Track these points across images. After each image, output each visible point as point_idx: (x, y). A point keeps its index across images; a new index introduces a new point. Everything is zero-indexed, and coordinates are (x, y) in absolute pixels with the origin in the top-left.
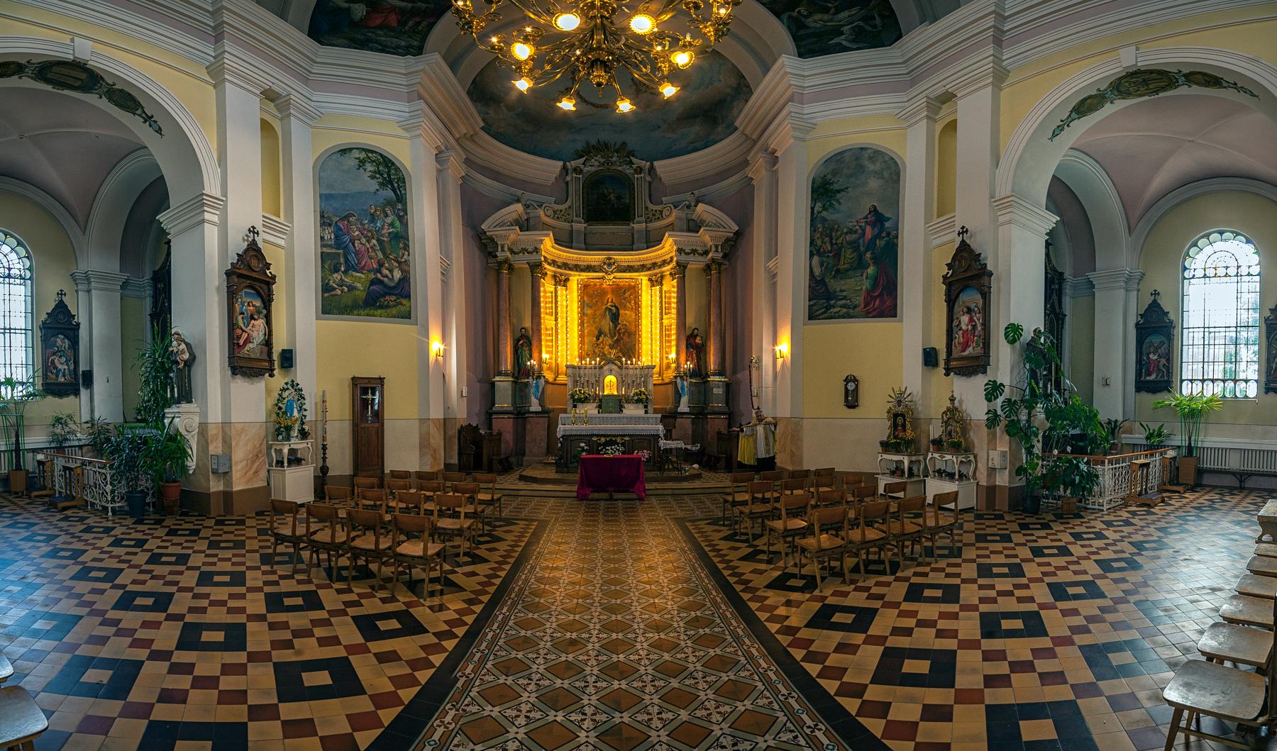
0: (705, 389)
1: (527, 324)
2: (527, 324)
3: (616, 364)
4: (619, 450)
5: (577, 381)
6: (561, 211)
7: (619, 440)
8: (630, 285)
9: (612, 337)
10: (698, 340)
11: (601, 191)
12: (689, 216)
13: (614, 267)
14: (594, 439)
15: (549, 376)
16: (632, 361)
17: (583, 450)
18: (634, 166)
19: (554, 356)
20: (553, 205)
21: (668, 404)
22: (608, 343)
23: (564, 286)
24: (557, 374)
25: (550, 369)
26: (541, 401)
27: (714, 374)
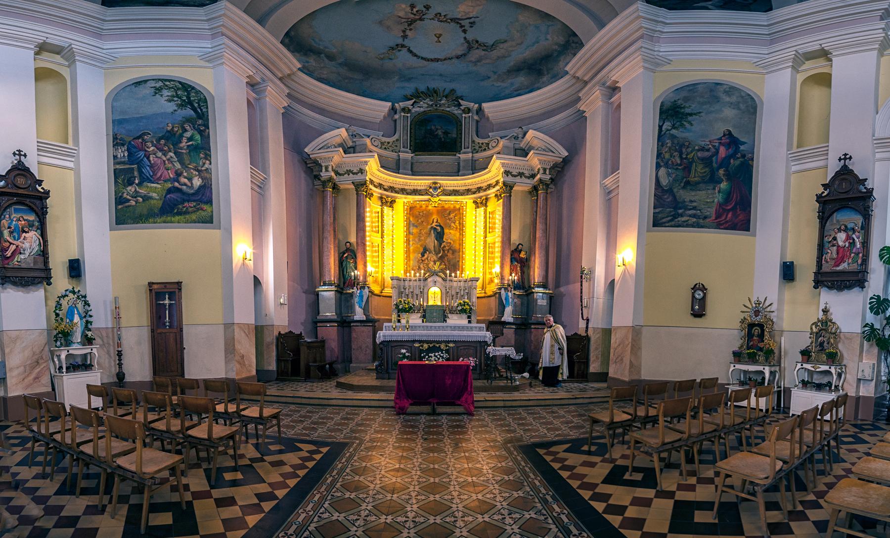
0: (528, 301)
1: (353, 239)
2: (353, 239)
3: (440, 277)
4: (443, 357)
5: (402, 293)
6: (389, 143)
7: (443, 346)
8: (454, 207)
9: (437, 254)
10: (522, 255)
11: (429, 128)
12: (517, 146)
13: (439, 191)
14: (417, 345)
15: (376, 289)
16: (456, 274)
17: (404, 357)
18: (462, 108)
19: (380, 270)
20: (381, 137)
21: (491, 316)
22: (432, 259)
23: (390, 207)
24: (383, 287)
25: (376, 281)
26: (366, 310)
27: (538, 287)
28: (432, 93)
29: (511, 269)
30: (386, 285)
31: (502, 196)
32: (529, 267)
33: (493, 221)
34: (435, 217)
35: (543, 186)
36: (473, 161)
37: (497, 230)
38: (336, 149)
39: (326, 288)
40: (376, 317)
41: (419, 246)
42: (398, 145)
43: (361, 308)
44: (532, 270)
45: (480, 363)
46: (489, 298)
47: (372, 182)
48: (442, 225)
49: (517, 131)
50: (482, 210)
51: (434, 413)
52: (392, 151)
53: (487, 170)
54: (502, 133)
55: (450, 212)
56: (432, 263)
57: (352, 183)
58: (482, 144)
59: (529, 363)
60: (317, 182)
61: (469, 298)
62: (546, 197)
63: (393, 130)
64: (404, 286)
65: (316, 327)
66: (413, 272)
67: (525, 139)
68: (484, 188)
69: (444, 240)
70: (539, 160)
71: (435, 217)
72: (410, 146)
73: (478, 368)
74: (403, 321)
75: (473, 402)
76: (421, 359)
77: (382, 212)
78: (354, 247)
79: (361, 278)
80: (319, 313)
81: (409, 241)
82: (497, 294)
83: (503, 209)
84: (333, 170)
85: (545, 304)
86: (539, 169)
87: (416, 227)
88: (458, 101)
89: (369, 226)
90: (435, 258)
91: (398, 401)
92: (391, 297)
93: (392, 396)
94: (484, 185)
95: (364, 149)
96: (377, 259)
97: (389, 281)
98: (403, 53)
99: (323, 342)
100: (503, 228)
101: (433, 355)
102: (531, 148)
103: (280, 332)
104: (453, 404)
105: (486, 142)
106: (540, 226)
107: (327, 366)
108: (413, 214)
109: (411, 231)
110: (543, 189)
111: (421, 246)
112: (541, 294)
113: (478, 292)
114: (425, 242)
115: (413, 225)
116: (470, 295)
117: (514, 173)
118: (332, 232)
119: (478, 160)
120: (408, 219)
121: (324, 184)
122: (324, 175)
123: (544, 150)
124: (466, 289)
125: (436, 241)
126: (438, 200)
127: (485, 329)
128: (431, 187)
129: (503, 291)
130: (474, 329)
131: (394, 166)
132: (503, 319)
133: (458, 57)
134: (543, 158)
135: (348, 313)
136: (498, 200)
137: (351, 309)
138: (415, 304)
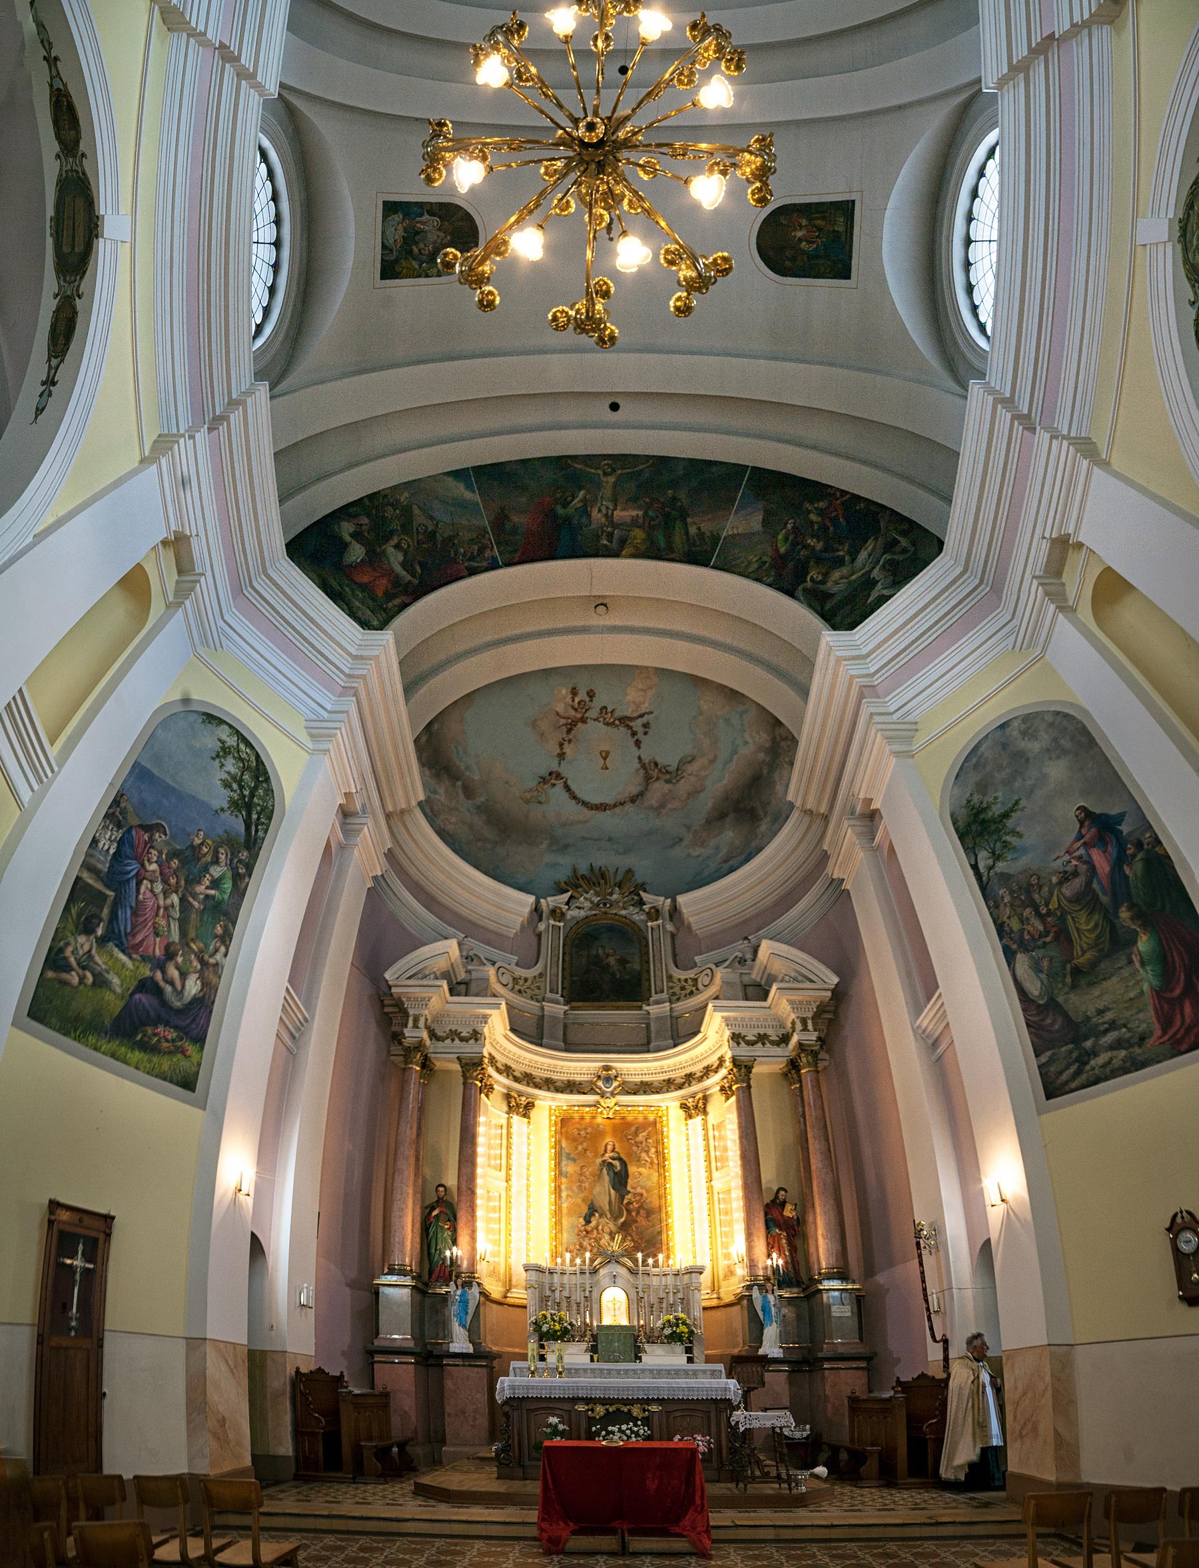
2: (451, 1180)
3: (624, 1265)
4: (637, 1435)
5: (547, 1298)
6: (526, 980)
7: (636, 1411)
8: (646, 1118)
9: (616, 1219)
10: (789, 1212)
12: (746, 979)
14: (581, 1408)
15: (495, 1291)
17: (555, 1432)
20: (513, 967)
21: (735, 1347)
22: (607, 1230)
26: (473, 1332)
28: (596, 879)
29: (768, 1244)
30: (514, 1282)
31: (734, 1088)
32: (805, 1238)
33: (722, 1144)
34: (609, 1140)
35: (806, 1056)
36: (674, 1019)
37: (731, 1164)
38: (438, 983)
39: (393, 1279)
40: (495, 1349)
41: (579, 1201)
42: (542, 985)
43: (464, 1326)
44: (811, 1242)
45: (720, 1450)
46: (729, 1309)
47: (492, 1060)
48: (622, 1156)
49: (739, 948)
50: (698, 1120)
51: (624, 1552)
52: (532, 998)
53: (700, 1036)
54: (715, 954)
55: (637, 1129)
56: (607, 1237)
57: (458, 1058)
58: (686, 980)
59: (825, 1447)
60: (396, 1049)
61: (686, 1310)
62: (818, 1081)
63: (535, 956)
64: (551, 1284)
65: (372, 1364)
66: (568, 1256)
67: (758, 961)
68: (699, 1074)
69: (629, 1188)
70: (791, 1002)
71: (609, 1140)
72: (563, 988)
73: (714, 1458)
74: (551, 1358)
75: (708, 1529)
76: (591, 1436)
77: (509, 1126)
78: (452, 1198)
79: (465, 1265)
80: (377, 1334)
81: (560, 1191)
82: (743, 1300)
83: (739, 1116)
84: (427, 1027)
85: (849, 1314)
86: (793, 1023)
87: (574, 1160)
88: (639, 895)
89: (483, 1155)
90: (612, 1226)
91: (545, 1525)
92: (525, 1307)
93: (533, 1516)
94: (697, 1069)
95: (484, 990)
96: (497, 1226)
97: (520, 1275)
98: (557, 793)
99: (386, 1395)
100: (744, 1157)
101: (615, 1429)
102: (771, 979)
103: (298, 1369)
104: (664, 1533)
105: (692, 976)
106: (815, 1146)
107: (395, 1449)
108: (567, 1132)
109: (564, 1169)
110: (809, 1064)
111: (583, 1200)
112: (836, 1294)
113: (705, 1297)
114: (591, 1194)
115: (569, 1157)
116: (688, 1303)
117: (750, 1038)
118: (412, 1160)
119: (681, 1016)
120: (558, 1143)
121: (408, 1052)
122: (411, 1034)
123: (795, 979)
124: (678, 1291)
125: (612, 1191)
126: (613, 1105)
127: (724, 1375)
128: (599, 1077)
129: (756, 1293)
130: (700, 1375)
131: (532, 1030)
132: (761, 1352)
133: (633, 800)
134: (796, 996)
135: (437, 1337)
136: (727, 1099)
137: (444, 1329)
138: (574, 1322)
